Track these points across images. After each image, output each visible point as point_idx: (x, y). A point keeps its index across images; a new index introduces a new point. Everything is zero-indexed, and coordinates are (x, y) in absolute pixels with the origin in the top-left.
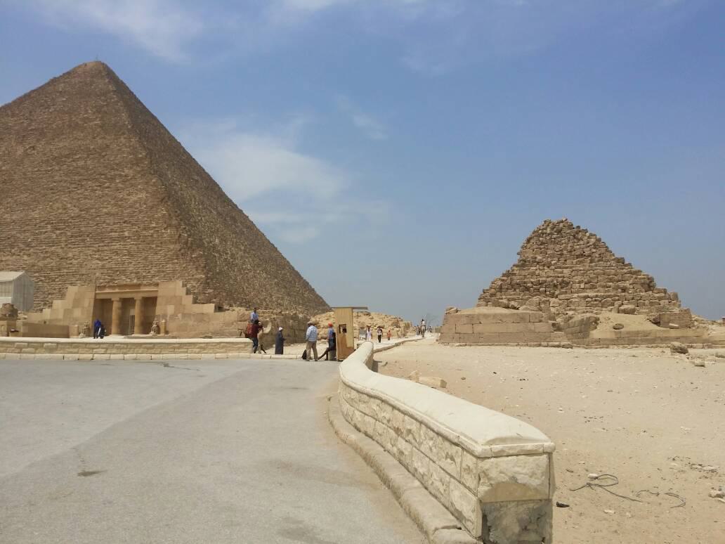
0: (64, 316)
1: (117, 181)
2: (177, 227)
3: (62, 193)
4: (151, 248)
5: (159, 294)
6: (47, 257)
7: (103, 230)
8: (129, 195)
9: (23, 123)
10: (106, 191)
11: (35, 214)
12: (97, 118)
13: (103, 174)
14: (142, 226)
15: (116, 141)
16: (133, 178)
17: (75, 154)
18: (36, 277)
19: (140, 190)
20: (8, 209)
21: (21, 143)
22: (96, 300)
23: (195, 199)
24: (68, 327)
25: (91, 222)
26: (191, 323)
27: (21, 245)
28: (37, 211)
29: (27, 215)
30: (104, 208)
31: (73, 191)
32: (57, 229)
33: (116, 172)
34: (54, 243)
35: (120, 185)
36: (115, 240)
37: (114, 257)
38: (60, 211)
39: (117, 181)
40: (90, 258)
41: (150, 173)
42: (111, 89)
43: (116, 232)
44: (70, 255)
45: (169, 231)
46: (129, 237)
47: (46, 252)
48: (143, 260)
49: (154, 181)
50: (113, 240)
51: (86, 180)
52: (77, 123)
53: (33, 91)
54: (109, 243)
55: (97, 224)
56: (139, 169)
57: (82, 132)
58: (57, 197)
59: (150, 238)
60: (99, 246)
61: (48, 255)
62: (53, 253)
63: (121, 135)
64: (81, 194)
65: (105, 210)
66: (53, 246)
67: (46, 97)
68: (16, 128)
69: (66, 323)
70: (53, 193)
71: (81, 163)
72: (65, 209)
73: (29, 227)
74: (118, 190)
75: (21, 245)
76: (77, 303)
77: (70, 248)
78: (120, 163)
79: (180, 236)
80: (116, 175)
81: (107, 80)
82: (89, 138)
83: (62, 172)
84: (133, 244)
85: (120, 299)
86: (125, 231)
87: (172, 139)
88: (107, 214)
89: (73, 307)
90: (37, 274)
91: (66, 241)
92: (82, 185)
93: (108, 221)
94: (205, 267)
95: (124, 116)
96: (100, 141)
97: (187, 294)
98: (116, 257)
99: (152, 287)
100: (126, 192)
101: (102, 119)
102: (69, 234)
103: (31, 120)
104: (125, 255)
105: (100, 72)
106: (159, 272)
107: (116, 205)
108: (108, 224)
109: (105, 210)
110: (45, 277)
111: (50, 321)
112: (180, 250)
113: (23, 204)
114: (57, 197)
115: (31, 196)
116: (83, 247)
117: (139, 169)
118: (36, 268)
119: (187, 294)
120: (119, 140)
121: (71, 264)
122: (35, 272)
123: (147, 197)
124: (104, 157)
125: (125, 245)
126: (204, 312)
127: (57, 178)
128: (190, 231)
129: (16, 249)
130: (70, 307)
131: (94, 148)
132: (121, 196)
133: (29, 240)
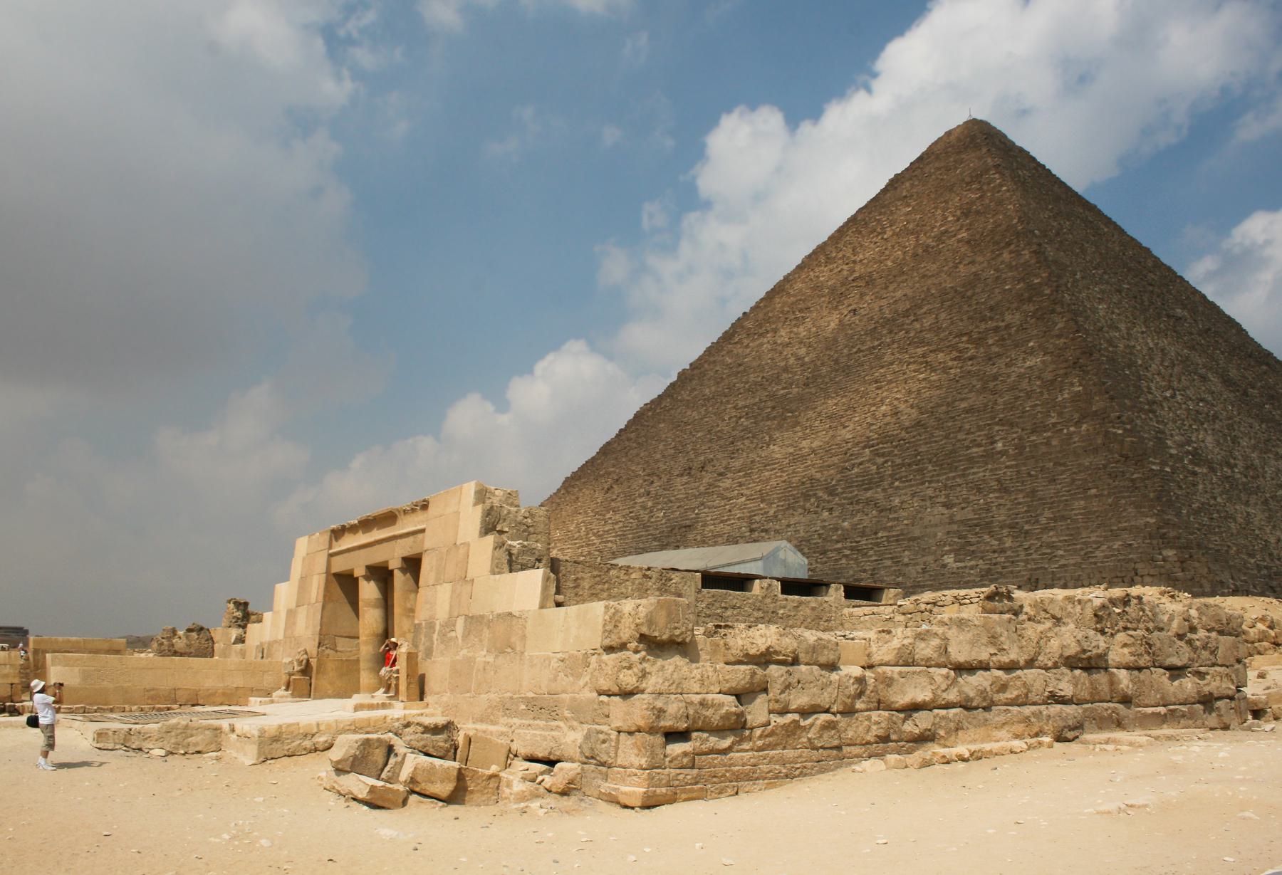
4: (1042, 470)
6: (858, 511)
18: (836, 550)
20: (808, 431)
25: (937, 433)
27: (820, 494)
30: (962, 400)
32: (878, 455)
36: (978, 462)
43: (979, 445)
45: (1084, 427)
46: (1002, 453)
47: (858, 502)
50: (971, 460)
51: (931, 351)
54: (965, 470)
55: (947, 437)
58: (885, 394)
59: (1044, 449)
60: (948, 479)
64: (924, 379)
70: (878, 388)
71: (927, 322)
73: (835, 459)
74: (990, 359)
77: (898, 488)
83: (895, 346)
88: (967, 411)
89: (297, 606)
92: (927, 362)
93: (967, 426)
100: (1001, 363)
102: (898, 461)
106: (1054, 519)
107: (984, 389)
109: (964, 405)
110: (852, 549)
112: (1105, 466)
113: (829, 417)
114: (885, 394)
115: (844, 400)
125: (996, 469)
126: (515, 610)
127: (887, 358)
128: (1131, 421)
129: (812, 500)
130: (293, 606)
132: (995, 370)
133: (834, 483)
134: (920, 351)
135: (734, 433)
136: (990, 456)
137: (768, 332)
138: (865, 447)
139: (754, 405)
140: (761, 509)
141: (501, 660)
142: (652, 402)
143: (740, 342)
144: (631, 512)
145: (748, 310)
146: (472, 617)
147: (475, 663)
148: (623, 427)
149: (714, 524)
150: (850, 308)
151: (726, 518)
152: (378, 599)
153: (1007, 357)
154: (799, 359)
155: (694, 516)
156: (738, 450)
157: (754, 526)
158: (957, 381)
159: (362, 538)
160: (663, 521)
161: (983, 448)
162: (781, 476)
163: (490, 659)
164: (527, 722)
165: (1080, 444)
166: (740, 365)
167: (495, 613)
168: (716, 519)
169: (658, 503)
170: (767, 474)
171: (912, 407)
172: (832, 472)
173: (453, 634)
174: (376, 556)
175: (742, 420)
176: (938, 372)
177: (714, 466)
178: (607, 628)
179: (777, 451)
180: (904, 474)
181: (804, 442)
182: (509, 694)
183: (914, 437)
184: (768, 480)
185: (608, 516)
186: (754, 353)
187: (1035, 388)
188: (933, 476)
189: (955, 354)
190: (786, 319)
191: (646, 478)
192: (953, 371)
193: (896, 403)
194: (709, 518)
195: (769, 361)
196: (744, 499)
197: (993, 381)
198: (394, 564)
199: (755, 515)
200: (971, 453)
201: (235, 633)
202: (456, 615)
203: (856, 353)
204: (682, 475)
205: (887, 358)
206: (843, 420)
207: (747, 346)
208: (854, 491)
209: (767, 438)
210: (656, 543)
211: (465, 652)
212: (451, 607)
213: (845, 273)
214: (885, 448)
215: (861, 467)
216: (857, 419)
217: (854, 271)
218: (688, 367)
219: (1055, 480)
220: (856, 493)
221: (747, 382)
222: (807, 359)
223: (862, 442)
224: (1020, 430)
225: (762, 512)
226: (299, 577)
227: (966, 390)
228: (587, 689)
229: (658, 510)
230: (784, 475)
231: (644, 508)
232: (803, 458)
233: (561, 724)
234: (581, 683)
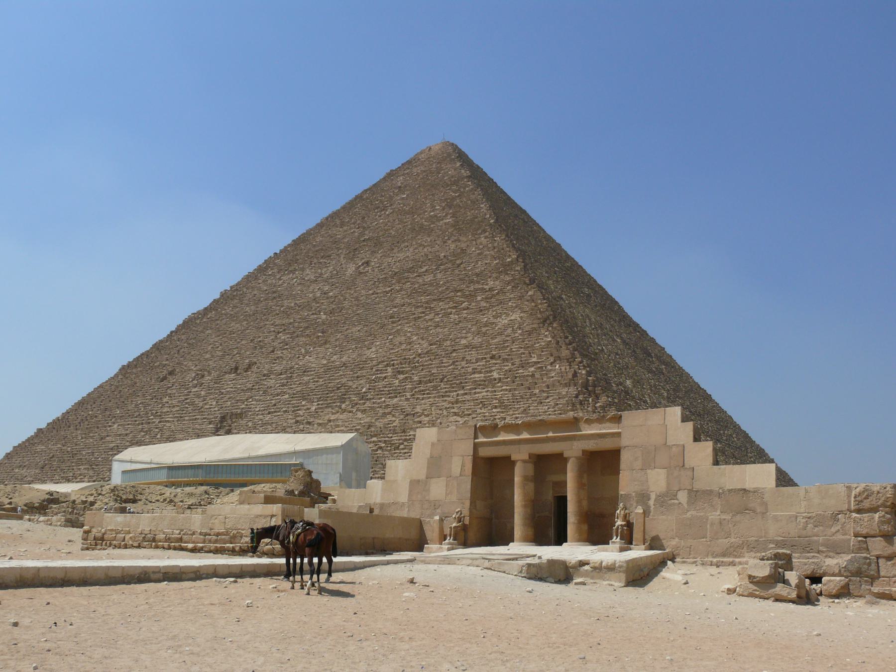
0: (410, 495)
1: (479, 298)
2: (570, 361)
3: (406, 321)
5: (625, 441)
7: (463, 370)
8: (495, 317)
9: (354, 232)
10: (464, 313)
11: (371, 353)
12: (446, 215)
13: (459, 291)
14: (517, 362)
15: (474, 243)
16: (502, 291)
17: (421, 267)
18: (374, 442)
19: (513, 309)
21: (352, 259)
22: (476, 458)
23: (590, 320)
24: (420, 525)
25: (445, 360)
26: (714, 516)
27: (354, 398)
28: (374, 349)
29: (360, 355)
30: (462, 338)
31: (419, 318)
32: (400, 373)
33: (477, 286)
34: (396, 393)
35: (483, 304)
36: (480, 385)
37: (479, 411)
38: (403, 347)
39: (479, 298)
40: (445, 413)
41: (525, 283)
42: (465, 174)
43: (480, 373)
44: (418, 409)
47: (387, 406)
48: (522, 413)
49: (530, 293)
50: (477, 384)
51: (434, 300)
52: (422, 224)
53: (366, 191)
54: (470, 389)
55: (454, 362)
56: (508, 278)
57: (429, 236)
58: (399, 327)
60: (458, 395)
61: (389, 410)
62: (395, 407)
63: (481, 234)
65: (463, 342)
66: (396, 397)
67: (382, 196)
68: (346, 240)
69: (415, 514)
70: (393, 322)
71: (429, 278)
72: (410, 343)
73: (364, 372)
75: (354, 398)
76: (435, 466)
77: (418, 399)
78: (482, 272)
79: (575, 375)
80: (476, 290)
81: (458, 164)
82: (438, 242)
84: (506, 390)
85: (530, 455)
86: (491, 371)
87: (549, 238)
88: (467, 347)
89: (427, 478)
90: (374, 439)
91: (412, 389)
92: (430, 308)
93: (468, 358)
96: (453, 246)
97: (696, 439)
98: (483, 411)
99: (608, 424)
101: (454, 215)
102: (416, 378)
103: (364, 228)
104: (496, 407)
105: (449, 155)
108: (468, 362)
109: (463, 342)
110: (385, 442)
111: (382, 506)
112: (577, 397)
114: (399, 327)
116: (435, 397)
117: (508, 278)
118: (373, 429)
120: (478, 242)
121: (420, 422)
122: (372, 436)
123: (521, 318)
124: (459, 266)
125: (495, 391)
126: (747, 486)
127: (398, 301)
128: (589, 366)
129: (347, 403)
130: (422, 476)
131: (445, 256)
132: (486, 319)
133: (364, 390)
134: (423, 299)
135: (275, 344)
136: (489, 382)
137: (295, 270)
138: (387, 365)
139: (290, 323)
140: (303, 406)
141: (738, 518)
142: (199, 313)
143: (273, 275)
144: (186, 399)
145: (278, 252)
146: (697, 491)
147: (707, 519)
148: (174, 329)
149: (263, 414)
150: (363, 261)
151: (272, 410)
152: (532, 476)
153: (493, 311)
154: (325, 294)
155: (243, 406)
156: (278, 357)
157: (298, 419)
158: (456, 324)
160: (216, 409)
161: (483, 375)
162: (317, 381)
165: (555, 378)
166: (274, 292)
167: (726, 489)
168: (264, 410)
169: (211, 393)
170: (305, 378)
171: (423, 339)
172: (362, 382)
173: (676, 501)
175: (280, 334)
176: (440, 316)
177: (258, 368)
178: (857, 499)
179: (311, 360)
180: (422, 388)
181: (334, 356)
183: (426, 361)
184: (307, 383)
185: (165, 400)
186: (286, 285)
187: (517, 335)
188: (446, 392)
189: (451, 304)
190: (311, 262)
192: (452, 316)
193: (409, 335)
194: (257, 409)
195: (299, 292)
196: (287, 396)
197: (485, 327)
199: (297, 410)
200: (474, 378)
202: (676, 489)
203: (373, 294)
204: (230, 373)
205: (398, 301)
206: (366, 343)
207: (280, 279)
208: (381, 398)
209: (303, 351)
210: (211, 426)
212: (668, 484)
213: (356, 234)
214: (403, 368)
215: (386, 380)
216: (378, 343)
217: (365, 234)
218: (229, 289)
219: (541, 403)
220: (383, 399)
221: (282, 306)
222: (331, 294)
223: (383, 362)
224: (510, 364)
225: (305, 408)
226: (428, 456)
227: (464, 331)
228: (838, 534)
229: (211, 399)
230: (321, 380)
231: (198, 396)
232: (337, 368)
233: (816, 555)
234: (833, 530)
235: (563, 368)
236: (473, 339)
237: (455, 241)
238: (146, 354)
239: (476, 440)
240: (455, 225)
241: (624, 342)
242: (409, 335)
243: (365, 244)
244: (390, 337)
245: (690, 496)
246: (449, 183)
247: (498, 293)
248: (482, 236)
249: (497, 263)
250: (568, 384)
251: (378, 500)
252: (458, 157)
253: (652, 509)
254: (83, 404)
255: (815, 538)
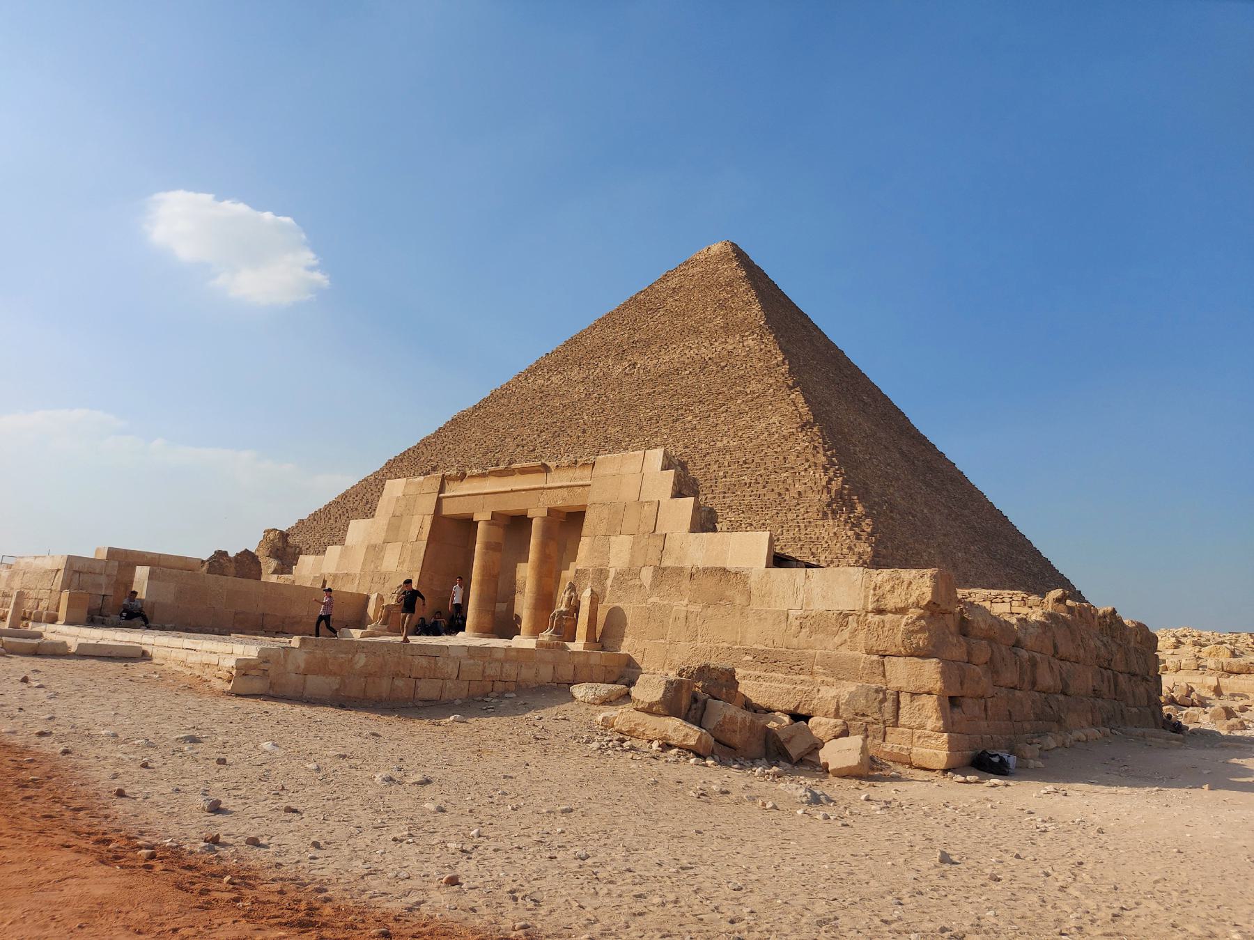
31: (678, 420)
49: (793, 396)
81: (735, 264)
87: (831, 345)
89: (386, 542)
94: (871, 534)
95: (756, 307)
97: (678, 493)
105: (727, 254)
109: (719, 444)
119: (678, 493)
126: (728, 566)
130: (380, 542)
141: (710, 611)
159: (492, 485)
163: (696, 608)
164: (757, 673)
173: (637, 582)
174: (512, 505)
182: (726, 645)
186: (553, 385)
191: (461, 469)
198: (537, 514)
201: (273, 564)
211: (654, 599)
227: (720, 435)
234: (837, 640)
235: (817, 475)
236: (728, 442)
237: (723, 343)
238: (413, 450)
239: (441, 495)
240: (725, 328)
241: (902, 453)
242: (665, 437)
243: (634, 345)
244: (647, 439)
245: (654, 577)
246: (723, 284)
247: (758, 397)
248: (749, 338)
249: (761, 366)
250: (821, 491)
251: (332, 570)
252: (736, 257)
253: (608, 592)
254: (346, 497)
255: (811, 651)
